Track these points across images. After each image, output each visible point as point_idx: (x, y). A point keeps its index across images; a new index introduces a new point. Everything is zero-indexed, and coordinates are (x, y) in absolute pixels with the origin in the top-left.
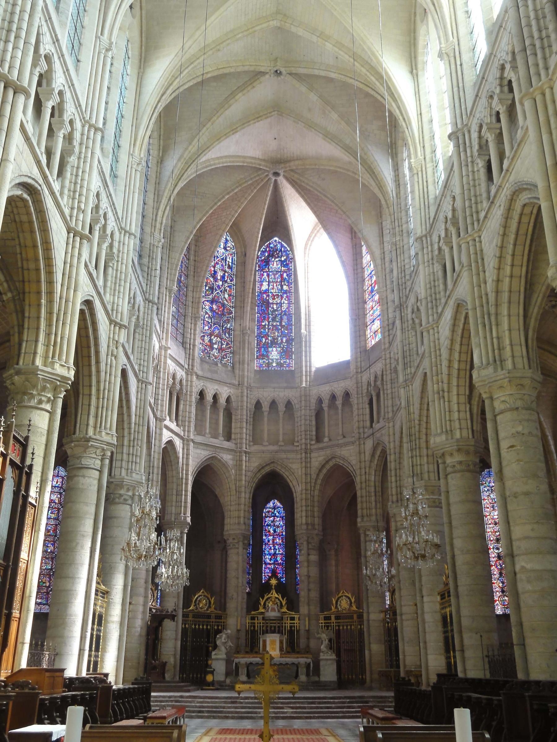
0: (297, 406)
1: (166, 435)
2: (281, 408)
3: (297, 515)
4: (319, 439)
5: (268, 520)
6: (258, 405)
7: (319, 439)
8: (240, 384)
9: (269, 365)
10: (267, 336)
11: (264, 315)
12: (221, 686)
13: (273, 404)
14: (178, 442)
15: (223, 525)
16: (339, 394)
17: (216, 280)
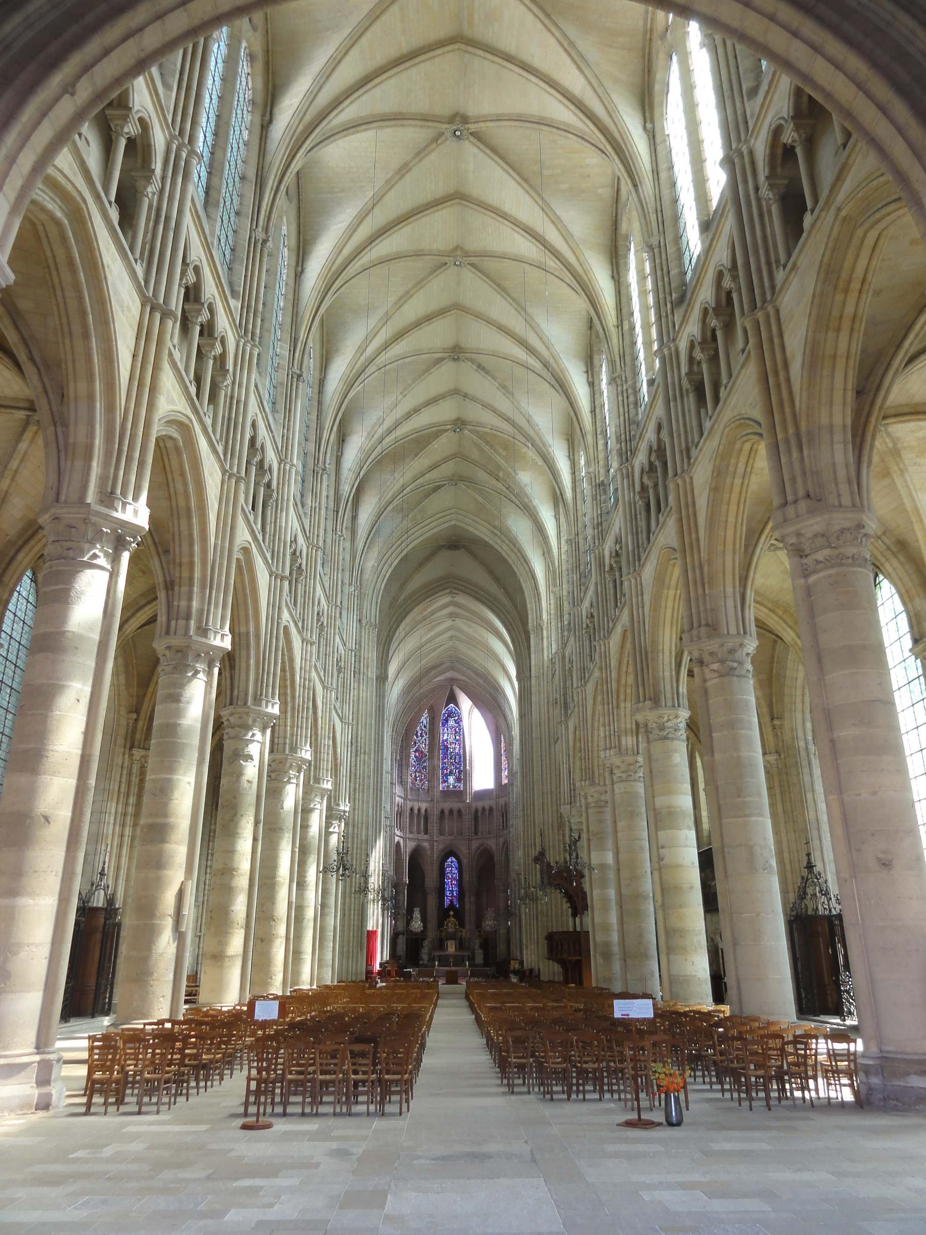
0: (464, 813)
1: (397, 839)
2: (455, 813)
3: (464, 875)
4: (476, 833)
5: (448, 870)
6: (442, 812)
7: (476, 833)
8: (432, 800)
9: (448, 787)
10: (447, 769)
11: (445, 755)
12: (426, 966)
13: (451, 811)
14: (401, 841)
15: (423, 881)
16: (487, 808)
17: (417, 737)
